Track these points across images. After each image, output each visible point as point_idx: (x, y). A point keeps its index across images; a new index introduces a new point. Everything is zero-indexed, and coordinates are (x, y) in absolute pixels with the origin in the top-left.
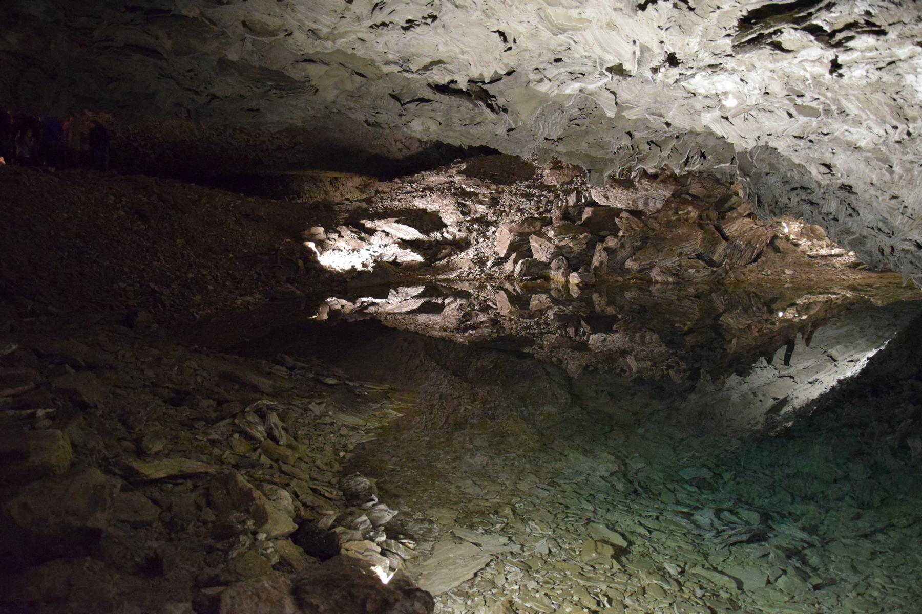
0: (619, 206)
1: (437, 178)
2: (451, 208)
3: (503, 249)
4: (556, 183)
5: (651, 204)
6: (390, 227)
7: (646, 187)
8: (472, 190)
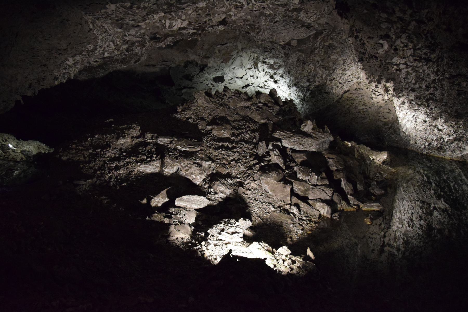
0: (314, 150)
1: (125, 140)
2: (194, 169)
3: (287, 196)
4: (228, 136)
5: (324, 146)
6: (182, 200)
7: (321, 136)
8: (188, 149)
